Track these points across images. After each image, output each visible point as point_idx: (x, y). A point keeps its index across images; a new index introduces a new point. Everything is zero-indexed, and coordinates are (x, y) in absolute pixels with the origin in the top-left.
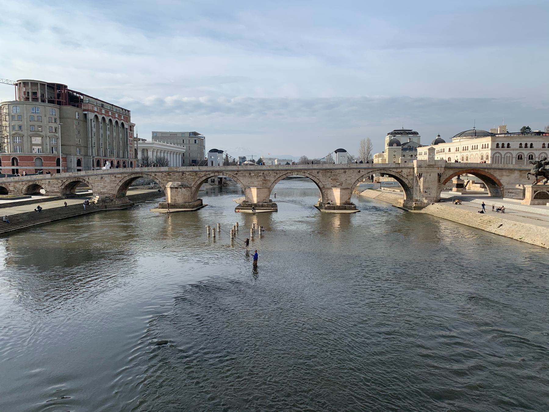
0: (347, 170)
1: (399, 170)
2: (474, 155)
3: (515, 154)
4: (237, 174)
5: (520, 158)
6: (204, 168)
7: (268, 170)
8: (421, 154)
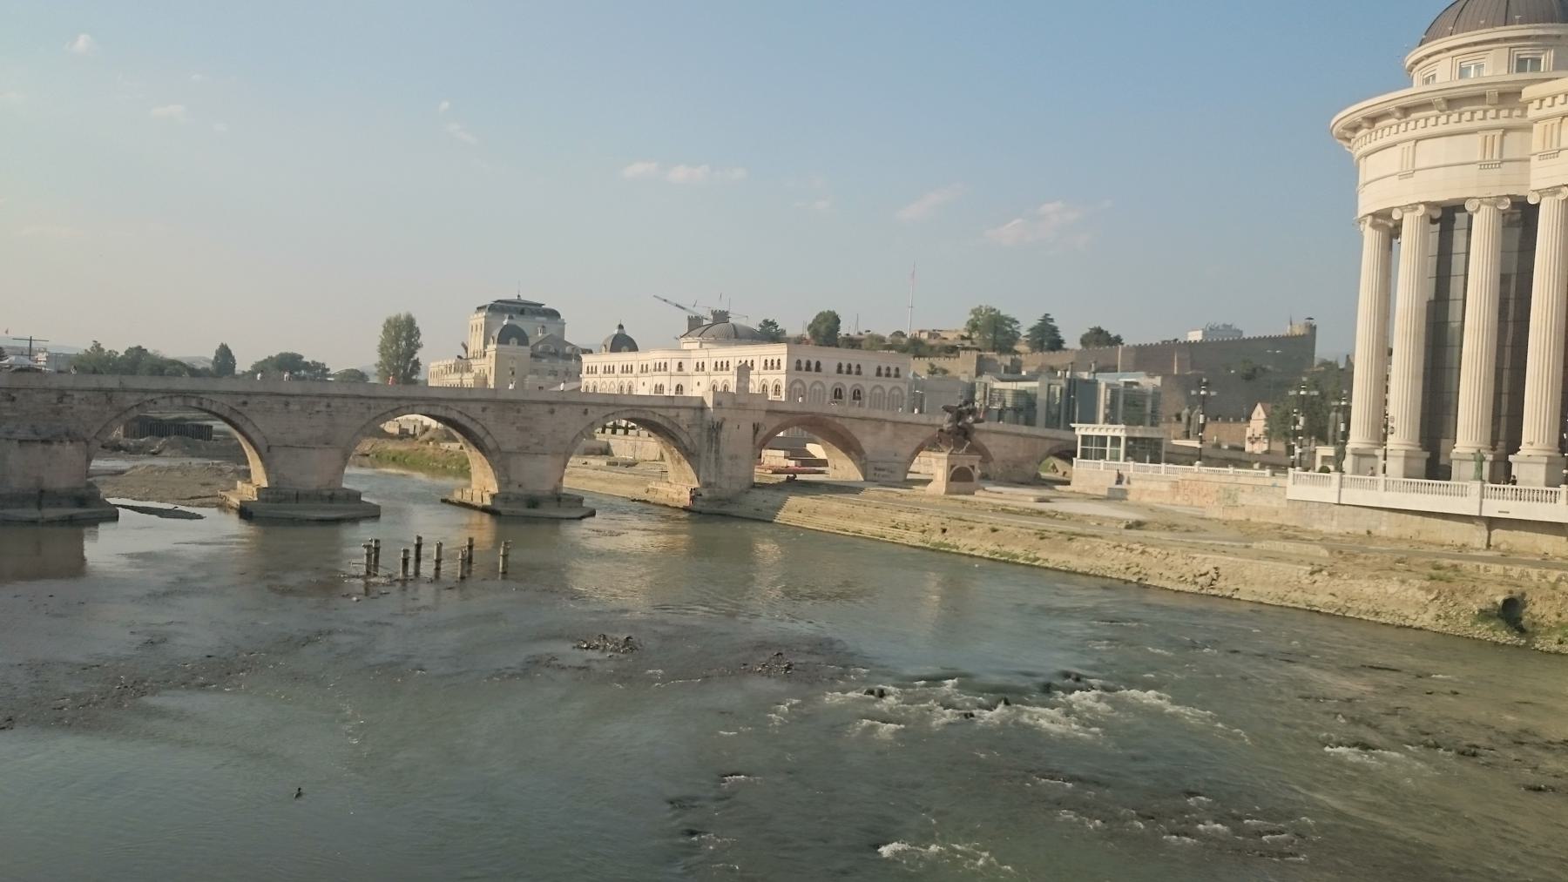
0: (556, 408)
1: (672, 413)
2: (887, 389)
3: (830, 384)
4: (245, 403)
5: (838, 394)
7: (344, 397)
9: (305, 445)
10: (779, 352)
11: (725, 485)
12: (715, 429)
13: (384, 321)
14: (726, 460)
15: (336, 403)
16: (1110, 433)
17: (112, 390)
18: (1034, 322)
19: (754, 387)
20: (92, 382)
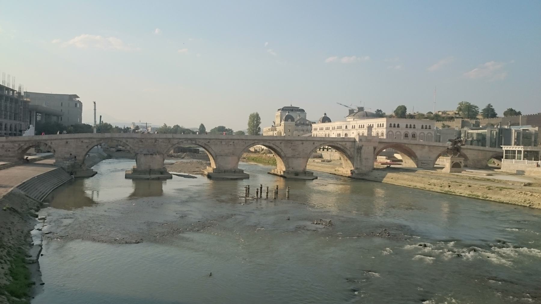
0: (304, 142)
1: (344, 143)
3: (403, 132)
4: (209, 142)
5: (406, 136)
6: (89, 135)
7: (238, 139)
8: (316, 129)
9: (227, 155)
10: (383, 121)
11: (364, 169)
12: (359, 149)
13: (249, 115)
14: (364, 160)
15: (236, 142)
16: (517, 149)
17: (170, 139)
18: (484, 107)
19: (374, 133)
20: (164, 136)
